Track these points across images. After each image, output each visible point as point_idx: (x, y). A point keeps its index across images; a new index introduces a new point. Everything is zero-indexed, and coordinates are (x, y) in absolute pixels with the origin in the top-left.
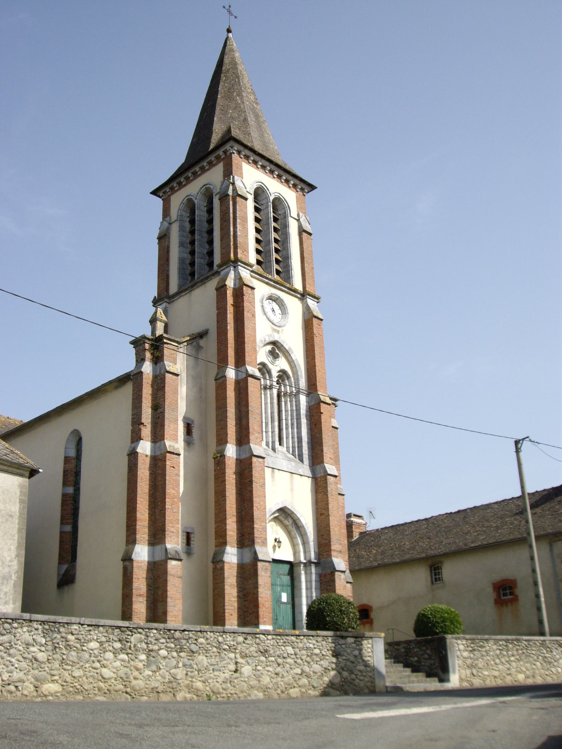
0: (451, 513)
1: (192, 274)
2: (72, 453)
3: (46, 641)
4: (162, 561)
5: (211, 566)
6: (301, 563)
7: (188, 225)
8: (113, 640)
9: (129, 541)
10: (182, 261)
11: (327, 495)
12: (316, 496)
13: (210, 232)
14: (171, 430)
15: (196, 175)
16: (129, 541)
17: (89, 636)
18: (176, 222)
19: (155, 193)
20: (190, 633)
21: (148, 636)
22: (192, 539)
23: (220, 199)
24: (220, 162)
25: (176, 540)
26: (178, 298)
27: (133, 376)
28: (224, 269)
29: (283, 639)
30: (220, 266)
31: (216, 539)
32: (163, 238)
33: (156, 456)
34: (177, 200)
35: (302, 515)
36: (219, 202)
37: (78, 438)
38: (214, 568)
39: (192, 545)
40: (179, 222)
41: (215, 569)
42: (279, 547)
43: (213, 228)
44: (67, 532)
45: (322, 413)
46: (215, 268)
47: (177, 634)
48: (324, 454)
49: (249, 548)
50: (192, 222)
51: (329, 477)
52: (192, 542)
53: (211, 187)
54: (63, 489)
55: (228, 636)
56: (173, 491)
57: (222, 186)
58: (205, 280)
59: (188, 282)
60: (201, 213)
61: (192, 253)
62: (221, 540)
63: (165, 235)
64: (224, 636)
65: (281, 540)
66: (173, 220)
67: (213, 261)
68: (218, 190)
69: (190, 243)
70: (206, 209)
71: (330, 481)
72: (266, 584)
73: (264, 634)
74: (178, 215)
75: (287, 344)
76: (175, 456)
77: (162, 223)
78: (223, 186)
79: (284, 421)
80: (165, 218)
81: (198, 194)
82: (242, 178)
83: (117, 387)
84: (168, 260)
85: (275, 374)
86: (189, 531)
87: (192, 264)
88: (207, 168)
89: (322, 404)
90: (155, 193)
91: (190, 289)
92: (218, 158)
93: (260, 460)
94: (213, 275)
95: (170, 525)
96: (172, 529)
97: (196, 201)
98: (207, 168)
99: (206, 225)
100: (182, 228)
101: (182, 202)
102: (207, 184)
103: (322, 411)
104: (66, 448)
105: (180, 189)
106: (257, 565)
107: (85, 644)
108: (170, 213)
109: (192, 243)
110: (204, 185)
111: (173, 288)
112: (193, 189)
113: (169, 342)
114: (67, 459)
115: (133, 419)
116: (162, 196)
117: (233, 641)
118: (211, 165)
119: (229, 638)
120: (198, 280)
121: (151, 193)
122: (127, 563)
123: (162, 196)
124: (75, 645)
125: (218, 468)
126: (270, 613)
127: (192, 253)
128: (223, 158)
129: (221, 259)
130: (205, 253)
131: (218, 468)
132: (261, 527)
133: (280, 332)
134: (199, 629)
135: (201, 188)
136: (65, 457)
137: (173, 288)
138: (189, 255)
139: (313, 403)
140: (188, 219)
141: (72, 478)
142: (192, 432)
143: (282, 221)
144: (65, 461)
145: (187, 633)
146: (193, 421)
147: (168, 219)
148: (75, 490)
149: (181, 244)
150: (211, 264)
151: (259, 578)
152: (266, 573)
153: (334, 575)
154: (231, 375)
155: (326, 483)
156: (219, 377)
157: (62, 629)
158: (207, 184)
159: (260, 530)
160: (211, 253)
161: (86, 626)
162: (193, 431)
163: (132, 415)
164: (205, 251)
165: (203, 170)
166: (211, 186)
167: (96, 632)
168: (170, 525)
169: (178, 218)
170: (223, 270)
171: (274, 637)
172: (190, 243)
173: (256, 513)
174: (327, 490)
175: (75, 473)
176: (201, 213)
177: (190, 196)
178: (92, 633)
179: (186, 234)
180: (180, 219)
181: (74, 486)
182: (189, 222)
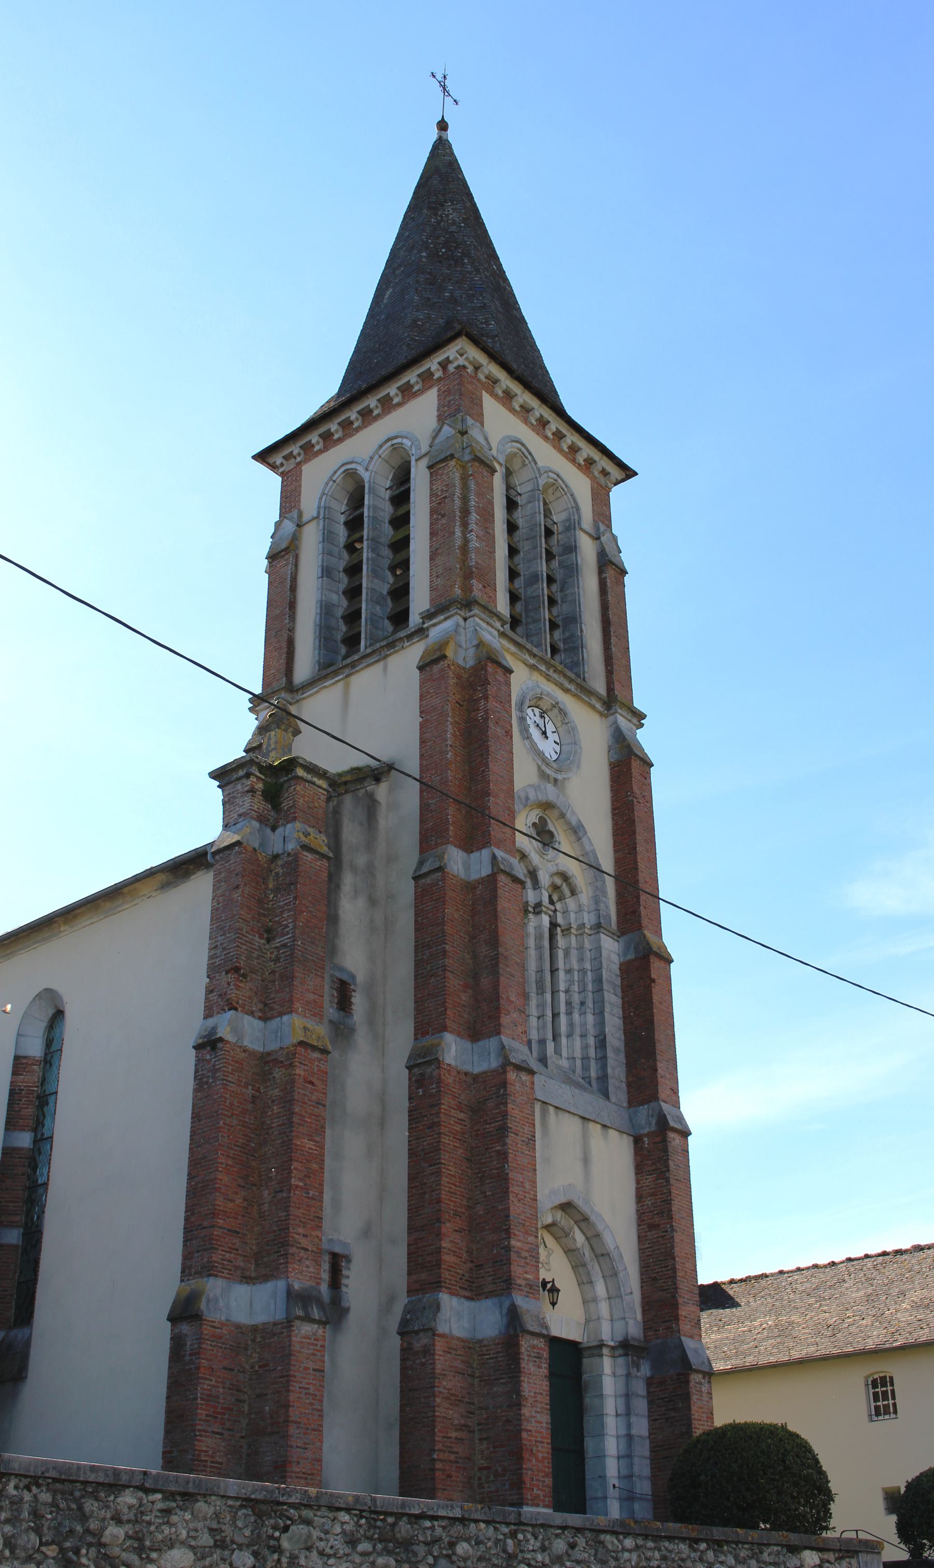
0: (816, 1266)
1: (352, 641)
2: (35, 1049)
3: (41, 1544)
4: (275, 1324)
5: (396, 1341)
6: (601, 1345)
7: (342, 533)
8: (233, 1542)
9: (190, 1267)
10: (326, 609)
11: (667, 1180)
12: (638, 1182)
13: (401, 545)
14: (308, 990)
15: (367, 416)
16: (190, 1267)
17: (167, 1530)
18: (315, 522)
19: (263, 457)
20: (436, 1523)
21: (327, 1532)
22: (345, 1272)
23: (430, 467)
24: (430, 387)
25: (311, 1269)
26: (317, 692)
27: (214, 854)
28: (440, 623)
29: (659, 1550)
30: (428, 616)
31: (409, 1274)
32: (282, 557)
33: (269, 1054)
34: (319, 473)
35: (607, 1226)
36: (427, 473)
37: (51, 1012)
38: (403, 1350)
39: (344, 1289)
40: (321, 522)
41: (406, 1352)
42: (553, 1304)
43: (409, 536)
44: (10, 1246)
45: (653, 981)
46: (415, 619)
47: (404, 1528)
48: (659, 1079)
49: (495, 1300)
50: (355, 524)
51: (671, 1135)
52: (344, 1281)
53: (407, 443)
54: (5, 1134)
55: (529, 1536)
56: (310, 1144)
57: (434, 438)
58: (387, 647)
59: (340, 658)
60: (377, 505)
61: (353, 593)
62: (423, 1276)
63: (287, 550)
64: (520, 1536)
65: (557, 1285)
66: (306, 518)
67: (407, 611)
68: (425, 448)
69: (346, 571)
70: (388, 493)
71: (673, 1143)
72: (539, 1398)
73: (614, 1533)
74: (319, 507)
75: (574, 813)
76: (316, 1055)
77: (278, 525)
78: (437, 441)
79: (562, 996)
80: (285, 513)
81: (372, 458)
82: (482, 425)
83: (165, 886)
84: (292, 605)
85: (544, 878)
86: (338, 1249)
87: (353, 617)
88: (396, 400)
89: (653, 959)
90: (263, 457)
91: (347, 671)
92: (427, 377)
93: (524, 1077)
94: (409, 637)
95: (301, 1230)
96: (304, 1242)
97: (366, 476)
98: (396, 400)
99: (388, 531)
100: (328, 537)
101: (331, 479)
102: (396, 437)
103: (653, 976)
104: (18, 1035)
105: (326, 449)
106: (517, 1345)
107: (154, 1555)
108: (299, 501)
109: (354, 570)
110: (389, 440)
111: (304, 668)
112: (363, 448)
113: (309, 777)
114: (20, 1064)
115: (210, 958)
116: (282, 465)
117: (543, 1549)
118: (408, 392)
119: (533, 1544)
120: (369, 651)
121: (254, 457)
122: (185, 1328)
123: (282, 465)
124: (124, 1556)
125: (421, 1092)
126: (546, 1476)
127: (353, 593)
128: (440, 379)
129: (431, 600)
130: (385, 592)
131: (421, 1092)
132: (527, 1247)
133: (559, 782)
134: (458, 1513)
135: (381, 446)
136: (17, 1058)
137: (304, 668)
138: (343, 598)
139: (631, 956)
140: (342, 519)
141: (30, 1111)
142: (351, 1003)
143: (560, 537)
144: (15, 1066)
145: (428, 1524)
146: (353, 977)
147: (295, 514)
148: (35, 1141)
149: (326, 572)
150: (400, 618)
151: (524, 1378)
152: (540, 1367)
153: (687, 1382)
154: (455, 868)
155: (665, 1150)
156: (425, 869)
157: (90, 1505)
158: (396, 437)
159: (524, 1254)
160: (401, 592)
161: (159, 1496)
162: (353, 1000)
163: (211, 949)
164: (385, 589)
165: (387, 405)
166: (405, 441)
167: (188, 1516)
168: (301, 1230)
169: (319, 513)
170: (434, 625)
171: (640, 1542)
172: (346, 571)
173: (516, 1209)
174: (668, 1166)
175: (38, 1097)
176: (377, 505)
177: (352, 462)
178: (174, 1519)
179: (337, 549)
180: (325, 514)
181: (35, 1130)
182: (346, 524)
